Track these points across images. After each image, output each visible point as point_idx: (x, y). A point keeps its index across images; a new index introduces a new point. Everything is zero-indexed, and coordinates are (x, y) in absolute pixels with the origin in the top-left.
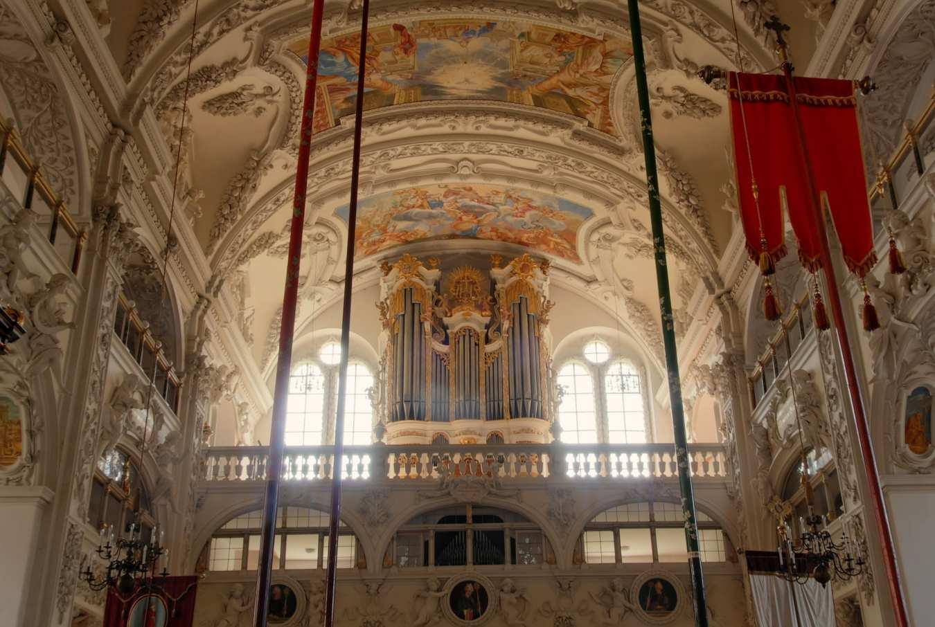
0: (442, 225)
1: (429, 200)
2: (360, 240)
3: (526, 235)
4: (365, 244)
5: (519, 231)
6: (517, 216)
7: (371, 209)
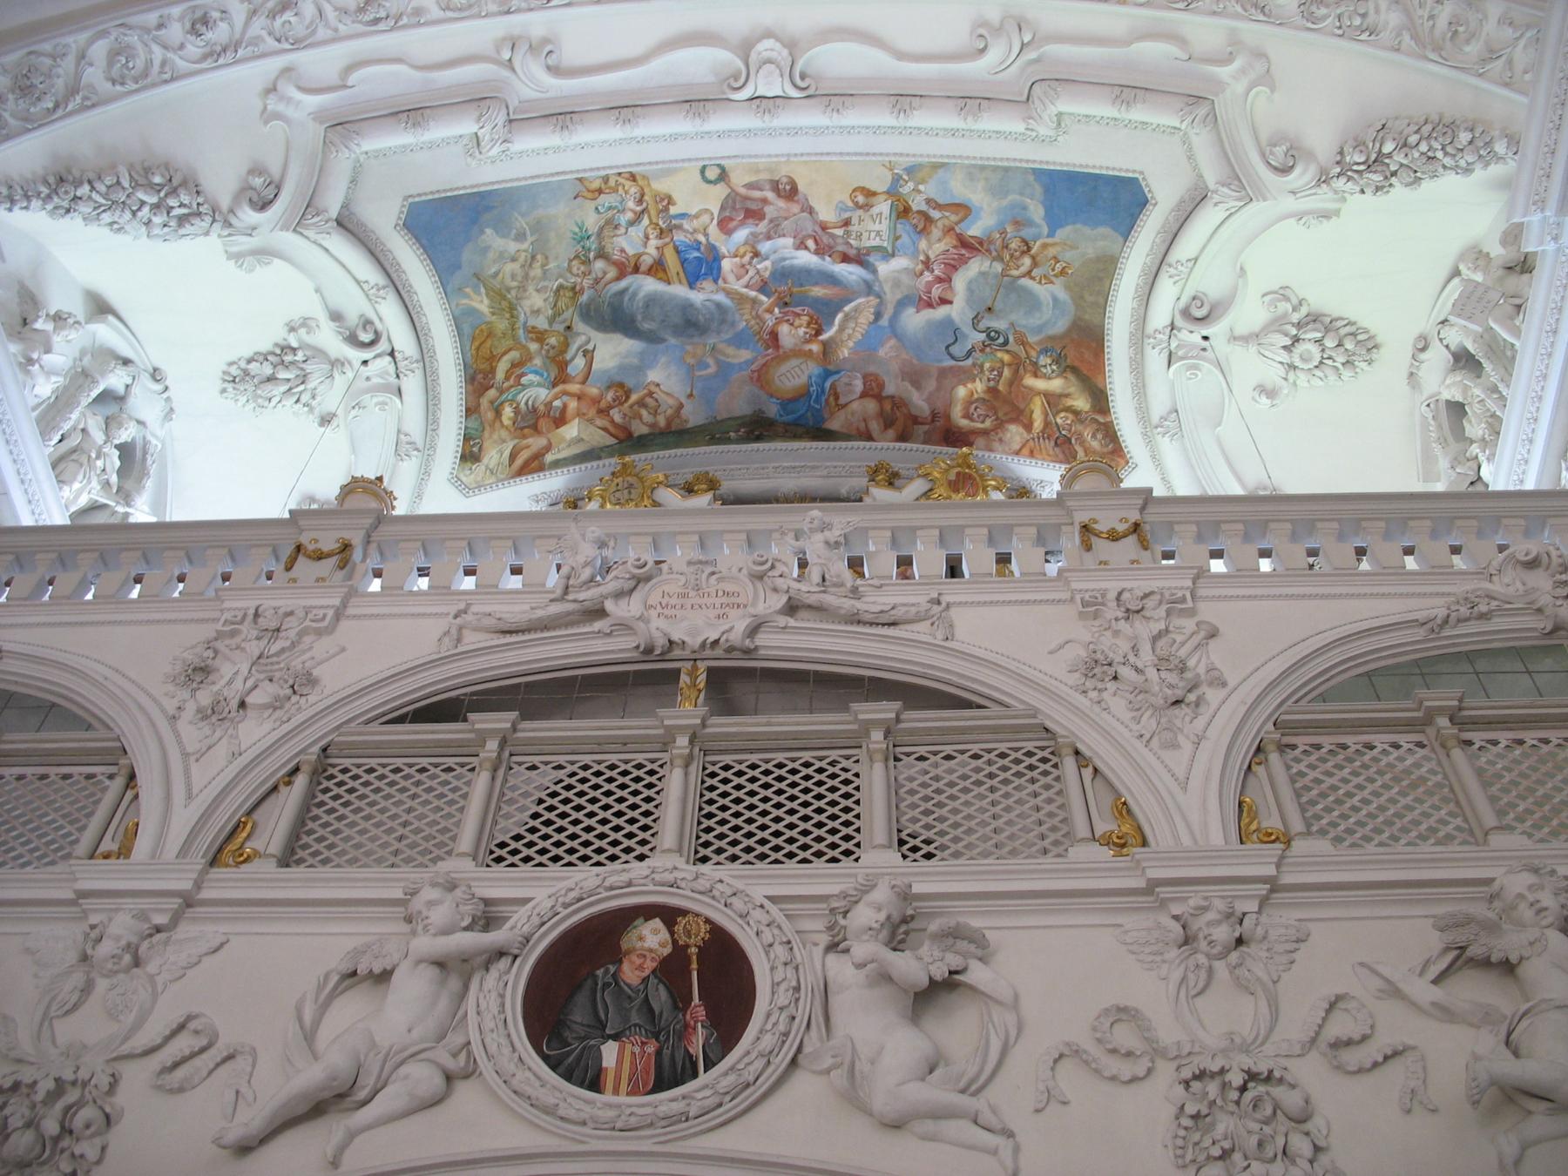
0: (724, 368)
1: (679, 237)
2: (492, 393)
3: (962, 392)
4: (508, 412)
5: (943, 373)
6: (930, 305)
7: (513, 247)
